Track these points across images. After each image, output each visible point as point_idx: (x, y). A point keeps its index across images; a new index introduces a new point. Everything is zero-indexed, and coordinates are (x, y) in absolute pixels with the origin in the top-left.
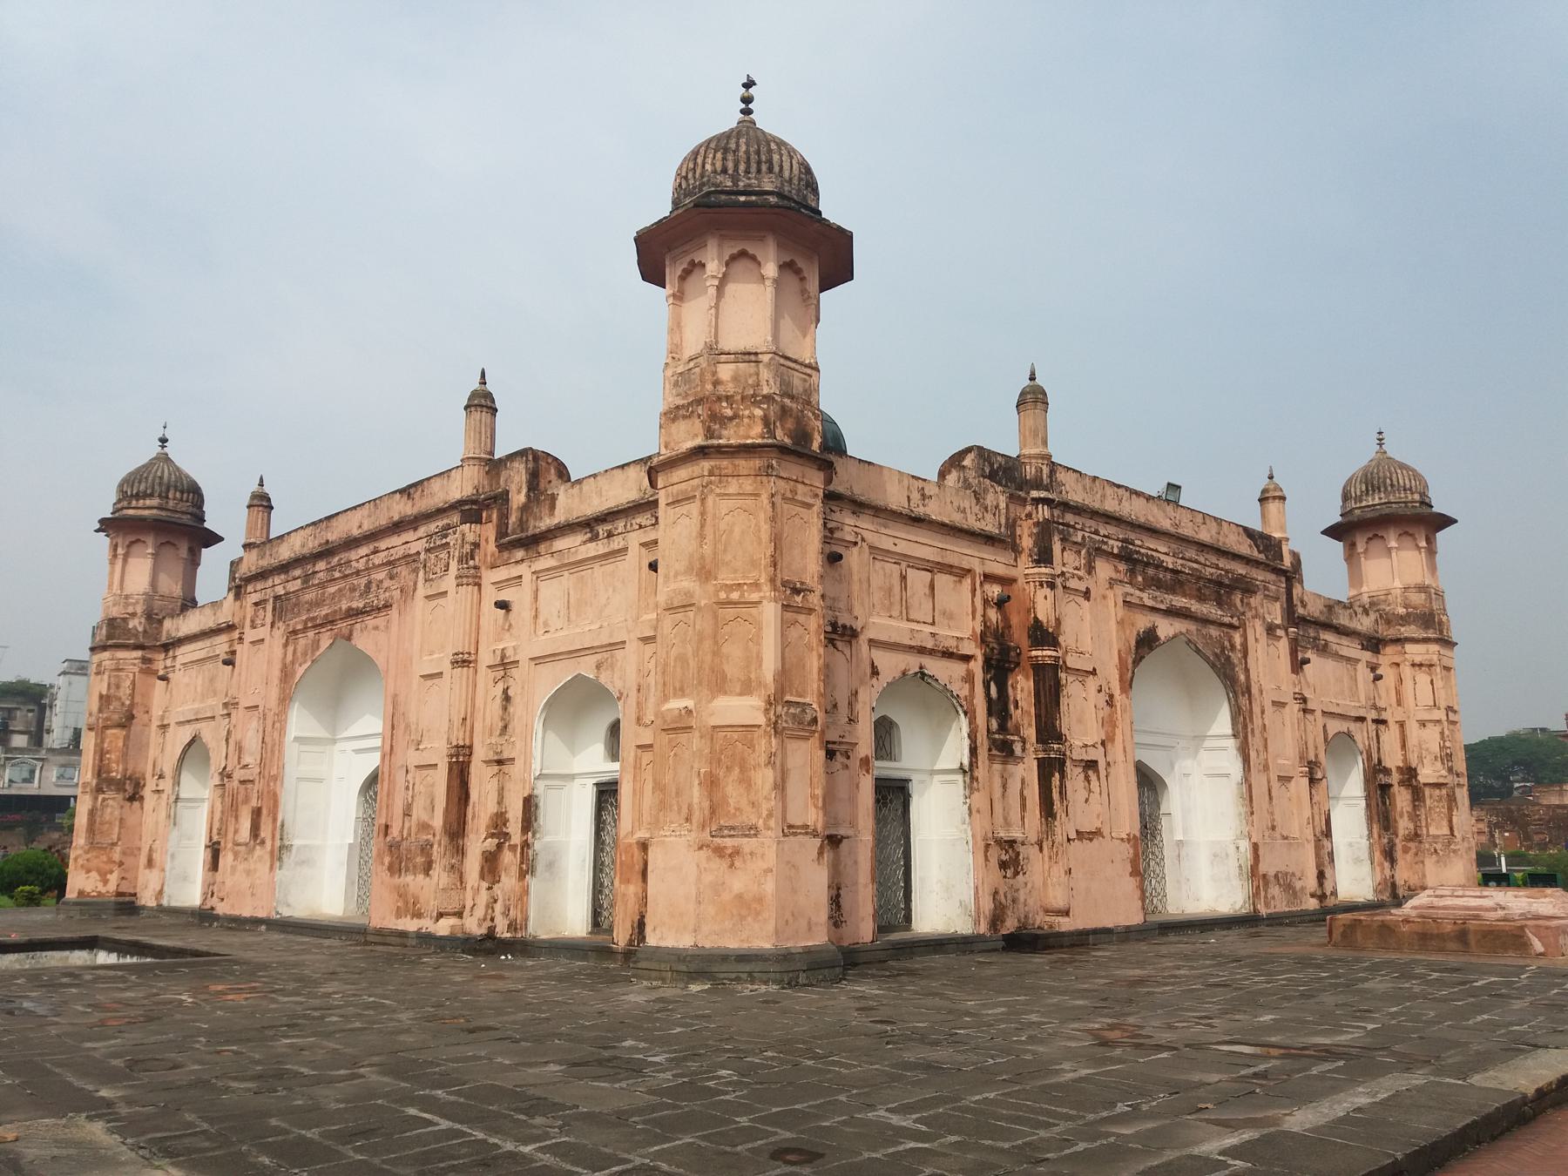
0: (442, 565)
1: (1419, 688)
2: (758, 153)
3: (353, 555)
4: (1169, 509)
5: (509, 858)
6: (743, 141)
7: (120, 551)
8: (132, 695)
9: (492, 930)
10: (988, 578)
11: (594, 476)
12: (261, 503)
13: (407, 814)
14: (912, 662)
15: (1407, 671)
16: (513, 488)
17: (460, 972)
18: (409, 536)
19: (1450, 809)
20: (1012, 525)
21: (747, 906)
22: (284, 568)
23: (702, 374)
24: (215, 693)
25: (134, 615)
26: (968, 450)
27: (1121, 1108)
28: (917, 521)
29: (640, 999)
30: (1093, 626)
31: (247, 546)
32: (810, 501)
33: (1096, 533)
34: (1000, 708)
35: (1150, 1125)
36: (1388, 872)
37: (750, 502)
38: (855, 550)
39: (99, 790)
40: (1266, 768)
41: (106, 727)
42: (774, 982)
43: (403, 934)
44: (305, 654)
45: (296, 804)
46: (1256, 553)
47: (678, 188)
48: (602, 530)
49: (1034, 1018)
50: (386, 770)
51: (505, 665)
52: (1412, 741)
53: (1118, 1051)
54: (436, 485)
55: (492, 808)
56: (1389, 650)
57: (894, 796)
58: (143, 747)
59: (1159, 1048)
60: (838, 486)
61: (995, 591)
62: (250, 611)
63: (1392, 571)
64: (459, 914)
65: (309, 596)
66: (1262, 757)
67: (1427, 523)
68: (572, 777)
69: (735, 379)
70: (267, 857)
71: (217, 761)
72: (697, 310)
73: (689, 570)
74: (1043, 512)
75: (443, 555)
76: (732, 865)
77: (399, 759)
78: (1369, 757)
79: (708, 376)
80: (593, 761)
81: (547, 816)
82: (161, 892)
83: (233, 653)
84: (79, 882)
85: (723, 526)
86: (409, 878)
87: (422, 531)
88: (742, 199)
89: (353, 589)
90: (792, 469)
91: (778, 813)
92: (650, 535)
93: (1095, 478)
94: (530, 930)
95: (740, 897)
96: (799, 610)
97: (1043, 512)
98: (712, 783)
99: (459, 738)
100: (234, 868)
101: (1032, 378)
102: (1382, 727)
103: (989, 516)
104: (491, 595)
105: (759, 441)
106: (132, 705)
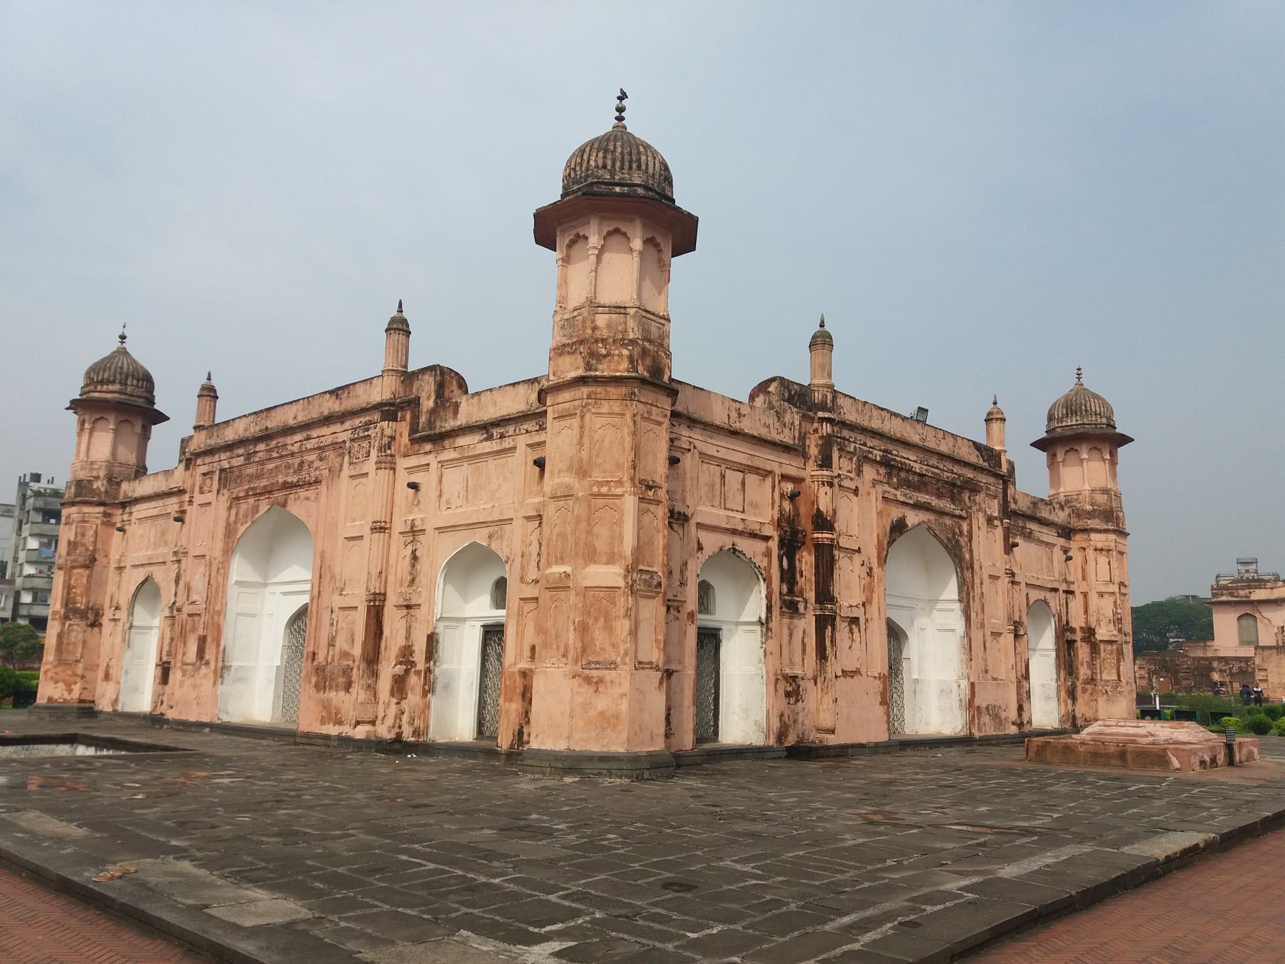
0: (364, 452)
1: (1100, 568)
2: (630, 154)
3: (289, 440)
4: (919, 427)
5: (414, 681)
6: (619, 144)
7: (87, 426)
8: (95, 542)
9: (399, 735)
10: (785, 477)
11: (491, 390)
12: (209, 393)
13: (331, 644)
14: (727, 541)
15: (1091, 554)
16: (424, 395)
17: (382, 767)
18: (337, 427)
19: (1119, 661)
20: (803, 437)
21: (607, 721)
22: (229, 447)
23: (584, 321)
24: (166, 543)
25: (97, 478)
26: (773, 380)
27: (889, 862)
28: (735, 434)
29: (530, 787)
30: (859, 515)
31: (195, 428)
32: (661, 419)
33: (865, 444)
34: (789, 576)
35: (910, 873)
36: (1070, 707)
37: (617, 420)
38: (689, 455)
39: (66, 617)
40: (983, 626)
41: (74, 568)
42: (627, 777)
43: (327, 737)
44: (246, 516)
45: (236, 634)
46: (981, 462)
47: (567, 177)
48: (496, 432)
49: (818, 805)
50: (314, 609)
51: (414, 532)
52: (1092, 608)
53: (882, 828)
54: (360, 389)
55: (401, 641)
56: (1078, 537)
57: (710, 640)
58: (103, 584)
59: (911, 826)
60: (679, 408)
61: (789, 487)
62: (199, 480)
63: (1083, 476)
64: (373, 723)
65: (251, 470)
66: (980, 617)
67: (1109, 440)
68: (464, 620)
69: (609, 326)
70: (211, 675)
71: (167, 595)
72: (580, 272)
73: (570, 469)
74: (827, 429)
75: (365, 444)
76: (597, 691)
77: (325, 601)
78: (1060, 619)
79: (588, 324)
80: (481, 608)
81: (445, 649)
82: (116, 700)
83: (184, 512)
84: (49, 690)
85: (596, 437)
86: (333, 694)
87: (348, 425)
88: (617, 189)
89: (288, 467)
90: (649, 395)
91: (631, 653)
92: (537, 438)
93: (865, 403)
94: (430, 735)
95: (602, 714)
96: (650, 502)
97: (827, 429)
98: (583, 629)
99: (376, 587)
100: (182, 684)
101: (822, 325)
102: (1070, 596)
103: (786, 431)
104: (403, 478)
105: (625, 374)
106: (95, 550)
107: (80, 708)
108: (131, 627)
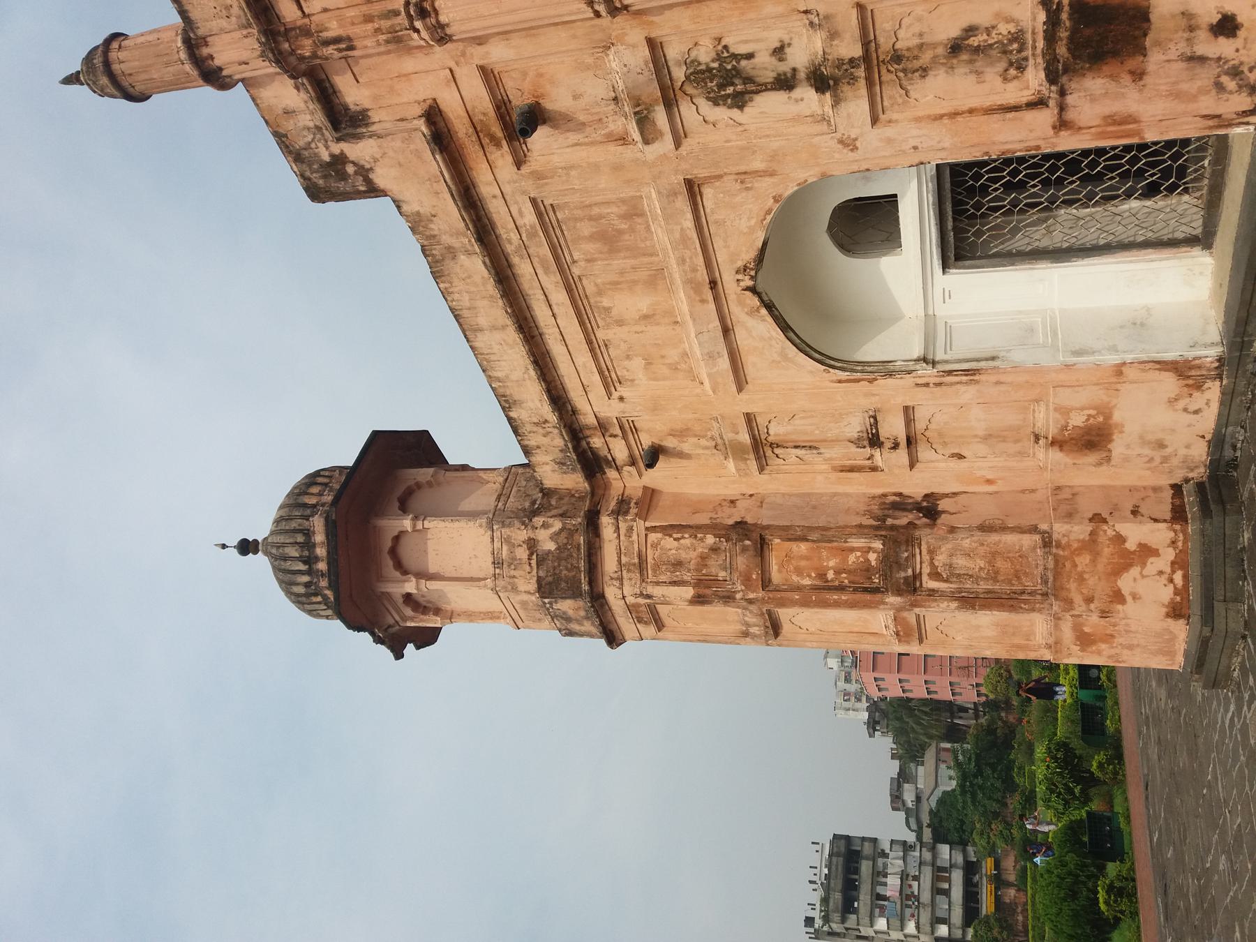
25: (532, 544)
39: (911, 587)
41: (766, 583)
82: (1181, 369)
106: (713, 528)
107: (1205, 512)
108: (925, 360)
